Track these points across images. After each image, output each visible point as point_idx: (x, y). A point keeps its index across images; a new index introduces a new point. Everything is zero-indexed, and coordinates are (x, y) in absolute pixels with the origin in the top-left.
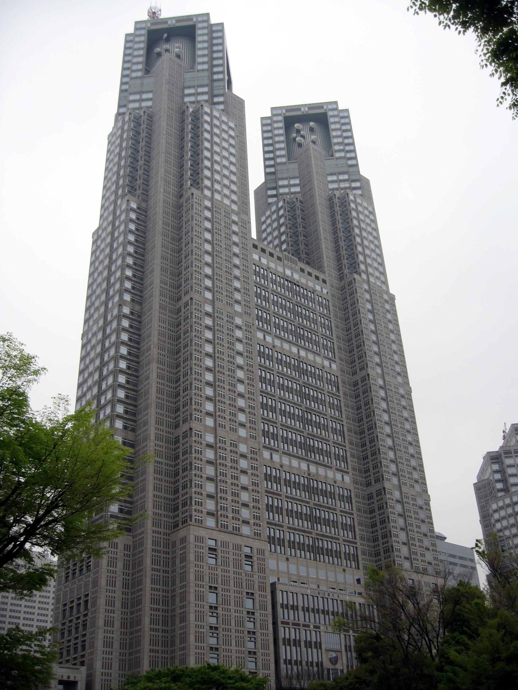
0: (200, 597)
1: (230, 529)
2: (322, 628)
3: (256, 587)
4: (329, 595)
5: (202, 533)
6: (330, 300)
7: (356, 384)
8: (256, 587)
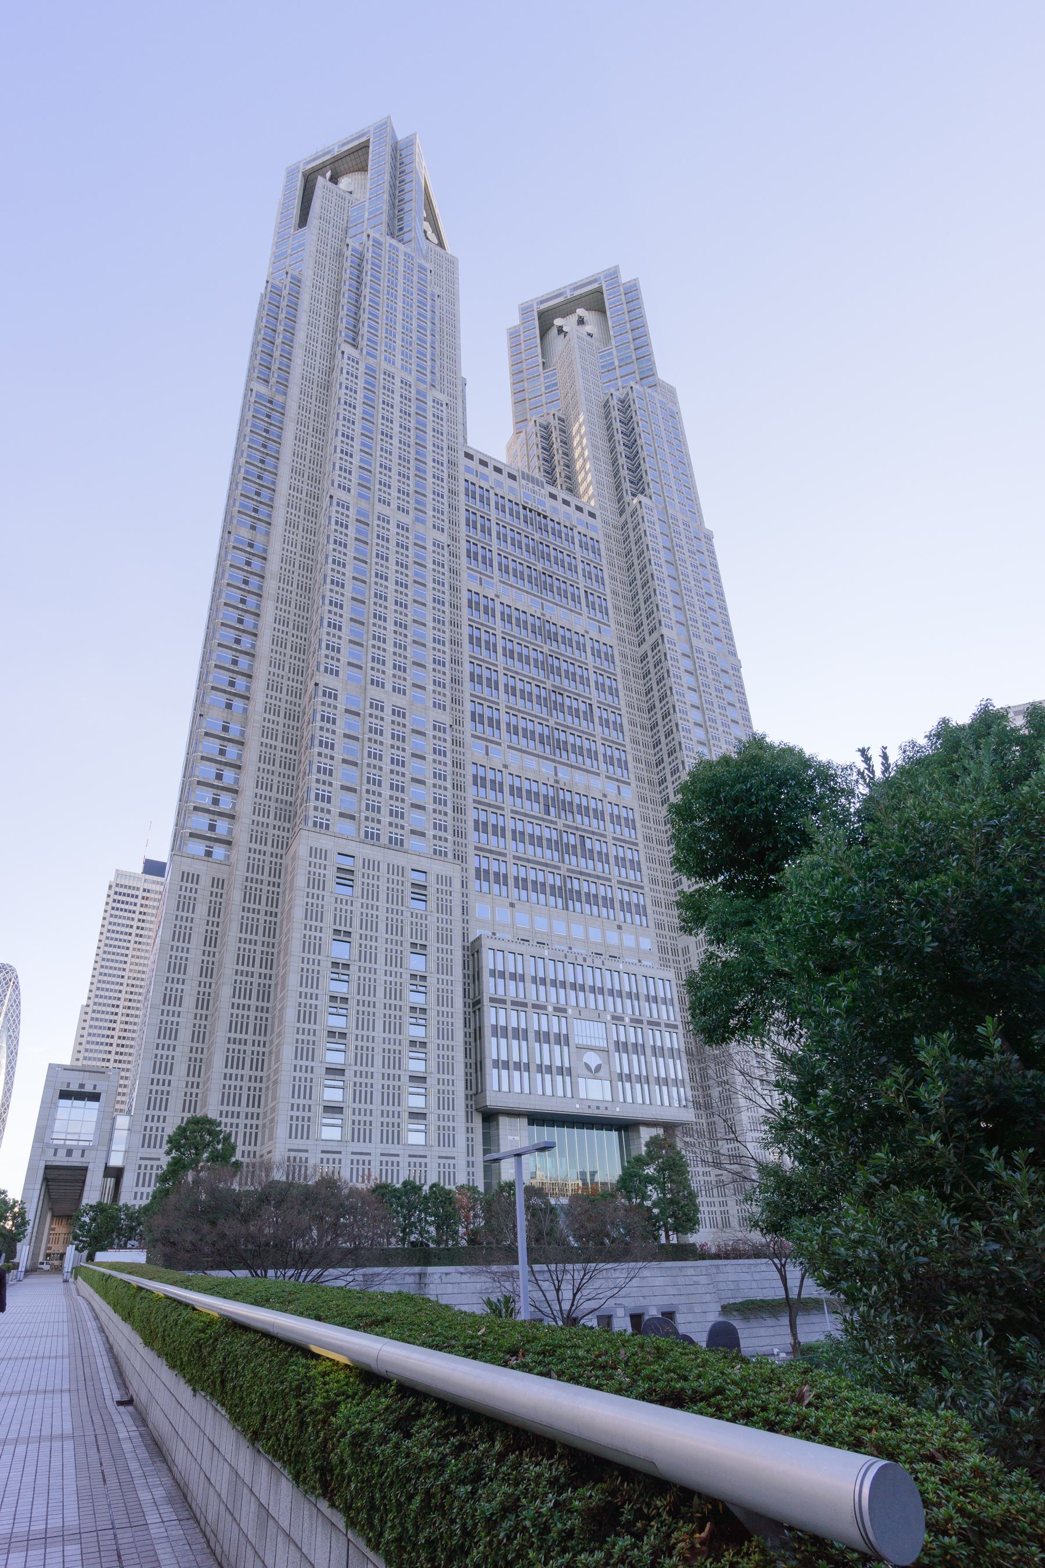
0: (313, 946)
1: (384, 840)
2: (570, 1011)
3: (432, 935)
4: (585, 960)
5: (324, 842)
6: (601, 540)
7: (645, 657)
8: (432, 935)
